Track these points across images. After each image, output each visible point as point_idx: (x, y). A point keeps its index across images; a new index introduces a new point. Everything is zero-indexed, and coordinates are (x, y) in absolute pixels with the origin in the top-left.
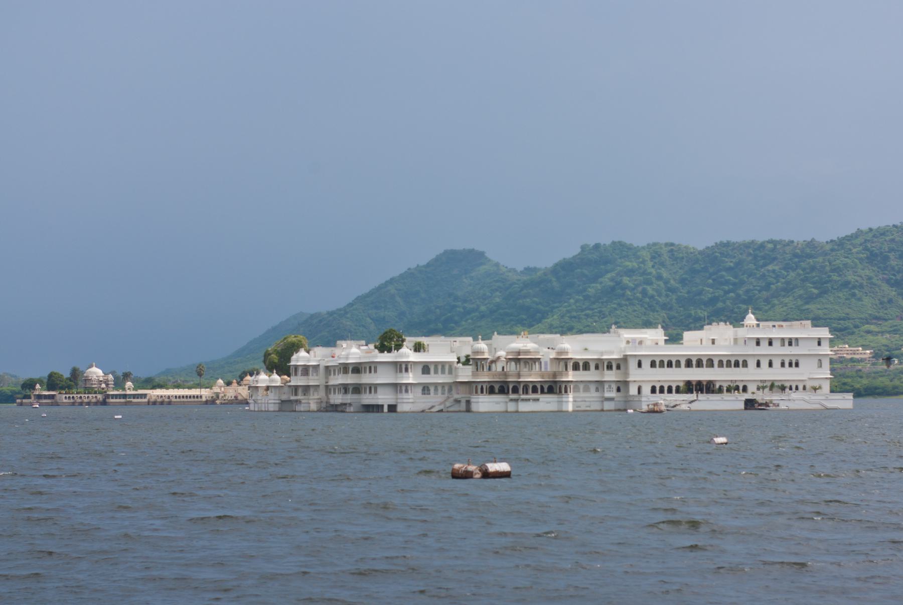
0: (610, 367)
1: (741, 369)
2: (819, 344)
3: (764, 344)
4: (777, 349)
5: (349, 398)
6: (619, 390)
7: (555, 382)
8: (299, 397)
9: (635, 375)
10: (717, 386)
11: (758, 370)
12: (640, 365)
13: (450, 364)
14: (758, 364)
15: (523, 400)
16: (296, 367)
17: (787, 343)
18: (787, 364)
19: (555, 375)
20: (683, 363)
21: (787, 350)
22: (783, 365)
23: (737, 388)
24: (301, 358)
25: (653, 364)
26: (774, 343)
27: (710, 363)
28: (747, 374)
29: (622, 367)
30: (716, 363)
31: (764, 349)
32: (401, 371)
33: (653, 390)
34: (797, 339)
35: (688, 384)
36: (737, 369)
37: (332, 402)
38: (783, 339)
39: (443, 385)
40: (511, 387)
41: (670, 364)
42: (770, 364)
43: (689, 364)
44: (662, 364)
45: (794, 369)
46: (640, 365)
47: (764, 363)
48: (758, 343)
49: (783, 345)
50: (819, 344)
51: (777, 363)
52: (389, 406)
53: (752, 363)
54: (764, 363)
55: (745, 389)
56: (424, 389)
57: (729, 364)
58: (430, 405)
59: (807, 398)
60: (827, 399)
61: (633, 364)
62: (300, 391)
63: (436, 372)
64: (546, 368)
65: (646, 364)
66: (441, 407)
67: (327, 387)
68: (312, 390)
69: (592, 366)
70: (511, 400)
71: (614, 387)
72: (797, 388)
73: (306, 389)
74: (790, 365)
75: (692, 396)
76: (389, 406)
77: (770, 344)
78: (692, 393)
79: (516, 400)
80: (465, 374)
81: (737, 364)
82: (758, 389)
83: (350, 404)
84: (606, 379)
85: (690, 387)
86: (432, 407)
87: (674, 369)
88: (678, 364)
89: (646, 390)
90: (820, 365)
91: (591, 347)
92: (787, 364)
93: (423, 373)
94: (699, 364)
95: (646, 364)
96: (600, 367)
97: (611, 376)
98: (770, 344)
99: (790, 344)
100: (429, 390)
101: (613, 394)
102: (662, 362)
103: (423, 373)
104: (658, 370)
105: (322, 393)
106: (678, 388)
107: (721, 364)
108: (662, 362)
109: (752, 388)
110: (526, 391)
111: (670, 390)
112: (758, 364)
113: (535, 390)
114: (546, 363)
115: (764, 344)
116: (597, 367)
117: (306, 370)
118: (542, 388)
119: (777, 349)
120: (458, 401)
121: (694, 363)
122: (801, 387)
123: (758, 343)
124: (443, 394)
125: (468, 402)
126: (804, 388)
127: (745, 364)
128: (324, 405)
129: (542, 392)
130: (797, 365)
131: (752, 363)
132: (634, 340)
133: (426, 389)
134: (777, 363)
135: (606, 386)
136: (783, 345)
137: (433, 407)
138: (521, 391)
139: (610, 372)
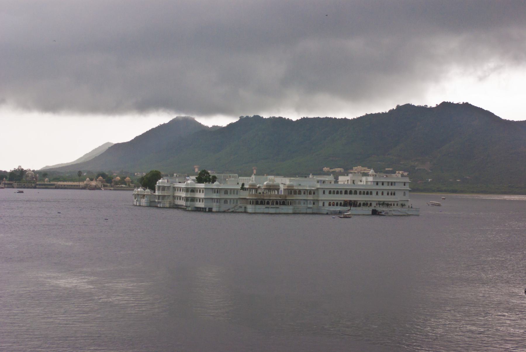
0: (310, 193)
1: (369, 195)
2: (405, 185)
3: (380, 184)
4: (386, 187)
5: (189, 203)
6: (314, 204)
7: (286, 200)
8: (160, 201)
10: (358, 204)
11: (377, 196)
12: (324, 193)
13: (237, 189)
14: (377, 194)
15: (271, 208)
16: (159, 187)
18: (390, 194)
19: (286, 197)
20: (343, 192)
22: (388, 194)
23: (367, 204)
24: (160, 182)
25: (330, 193)
26: (384, 184)
27: (356, 193)
28: (373, 198)
29: (316, 193)
30: (358, 192)
31: (380, 187)
32: (215, 192)
34: (395, 182)
35: (345, 201)
37: (176, 203)
38: (388, 182)
39: (234, 199)
40: (266, 201)
41: (337, 193)
42: (382, 194)
43: (346, 193)
45: (393, 196)
46: (324, 193)
47: (380, 193)
48: (377, 184)
50: (405, 185)
51: (385, 193)
52: (209, 208)
53: (374, 193)
54: (380, 193)
55: (371, 204)
56: (225, 201)
57: (364, 193)
58: (227, 208)
59: (399, 210)
60: (408, 210)
61: (321, 192)
62: (161, 198)
63: (231, 193)
64: (281, 193)
65: (327, 192)
66: (233, 210)
67: (174, 196)
68: (166, 197)
69: (302, 193)
70: (266, 208)
71: (312, 202)
72: (394, 205)
73: (164, 197)
74: (391, 194)
75: (348, 208)
76: (209, 208)
77: (383, 184)
78: (347, 206)
79: (268, 208)
80: (245, 195)
81: (367, 193)
82: (377, 205)
83: (189, 207)
84: (309, 198)
85: (346, 203)
86: (229, 209)
87: (339, 195)
88: (341, 193)
89: (327, 204)
90: (405, 194)
91: (302, 184)
92: (390, 194)
93: (225, 194)
94: (351, 193)
95: (327, 192)
96: (306, 193)
97: (310, 197)
98: (383, 184)
99: (392, 185)
101: (311, 206)
103: (225, 194)
104: (332, 195)
105: (171, 199)
106: (341, 203)
107: (360, 193)
108: (334, 192)
109: (374, 204)
110: (273, 204)
111: (337, 205)
112: (377, 194)
113: (277, 203)
114: (281, 191)
115: (380, 184)
116: (304, 193)
117: (164, 188)
118: (280, 203)
119: (386, 187)
120: (241, 207)
121: (348, 192)
122: (396, 205)
123: (377, 184)
124: (233, 203)
125: (245, 208)
126: (397, 205)
127: (371, 193)
128: (172, 205)
129: (280, 204)
130: (394, 194)
131: (374, 193)
132: (321, 180)
133: (226, 201)
134: (385, 193)
135: (309, 202)
137: (229, 209)
138: (270, 204)
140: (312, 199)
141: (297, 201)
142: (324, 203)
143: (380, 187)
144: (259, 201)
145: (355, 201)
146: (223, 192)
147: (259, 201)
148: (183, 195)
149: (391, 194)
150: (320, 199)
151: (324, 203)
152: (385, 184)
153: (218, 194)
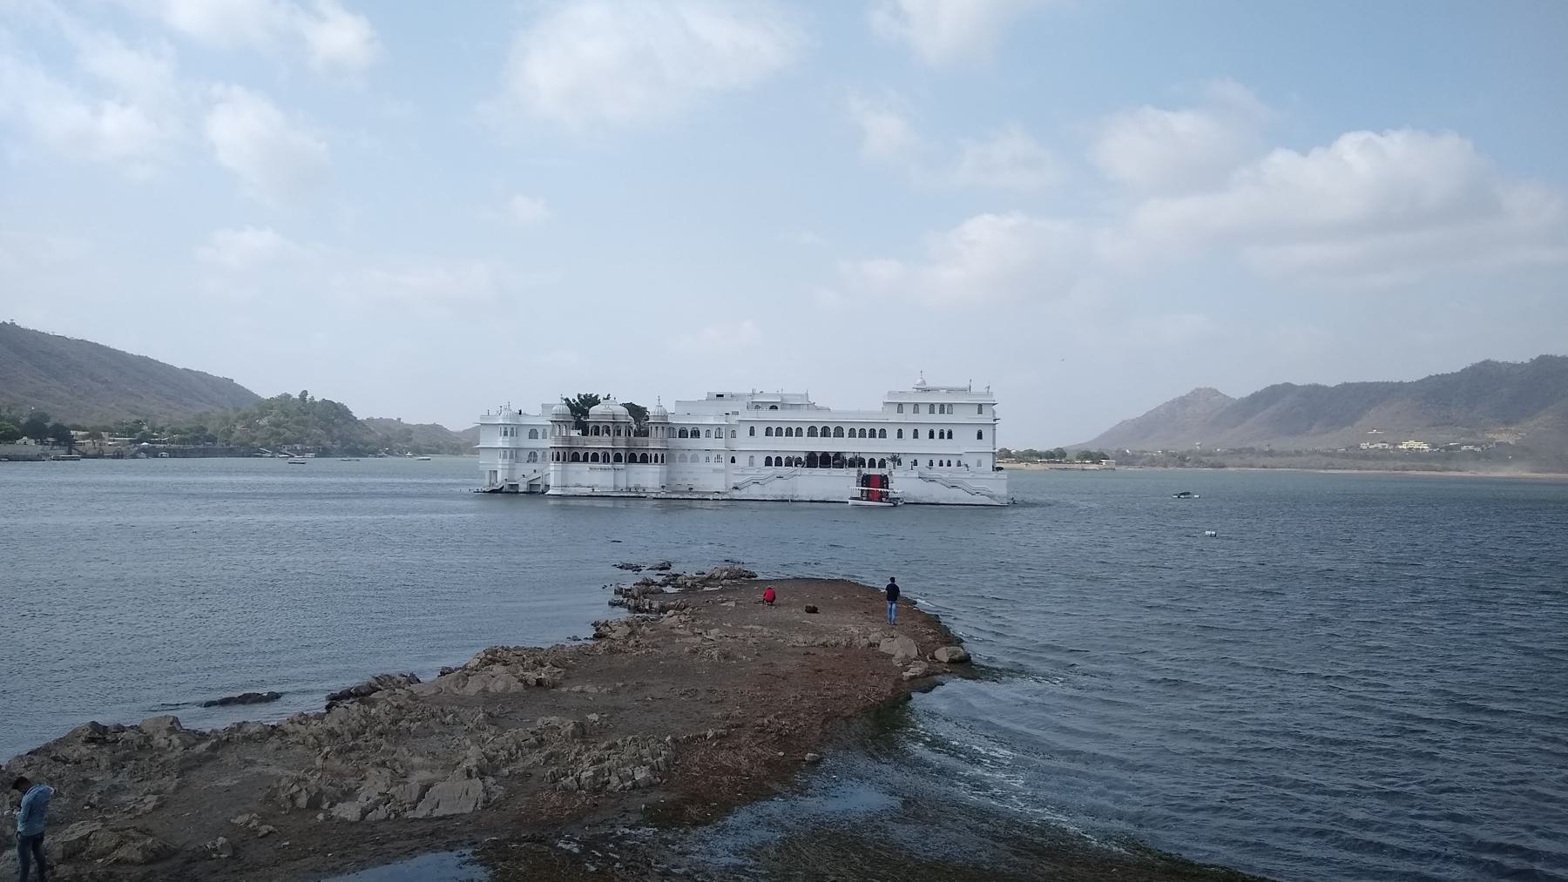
2: (980, 412)
3: (908, 410)
4: (924, 416)
12: (752, 433)
17: (937, 409)
18: (937, 435)
20: (805, 431)
21: (937, 418)
22: (932, 435)
25: (768, 432)
27: (839, 432)
30: (846, 432)
31: (909, 416)
33: (768, 462)
38: (932, 405)
41: (789, 432)
42: (916, 435)
43: (812, 432)
46: (752, 433)
47: (908, 433)
49: (932, 411)
50: (980, 412)
51: (924, 433)
53: (892, 433)
54: (908, 433)
57: (862, 433)
65: (760, 430)
69: (702, 434)
74: (942, 436)
81: (873, 434)
88: (799, 432)
92: (937, 435)
97: (719, 444)
102: (779, 430)
107: (852, 433)
108: (779, 430)
115: (908, 410)
119: (924, 416)
122: (954, 463)
127: (883, 434)
130: (950, 436)
131: (892, 433)
134: (924, 433)
136: (932, 411)
143: (909, 416)
148: (501, 442)
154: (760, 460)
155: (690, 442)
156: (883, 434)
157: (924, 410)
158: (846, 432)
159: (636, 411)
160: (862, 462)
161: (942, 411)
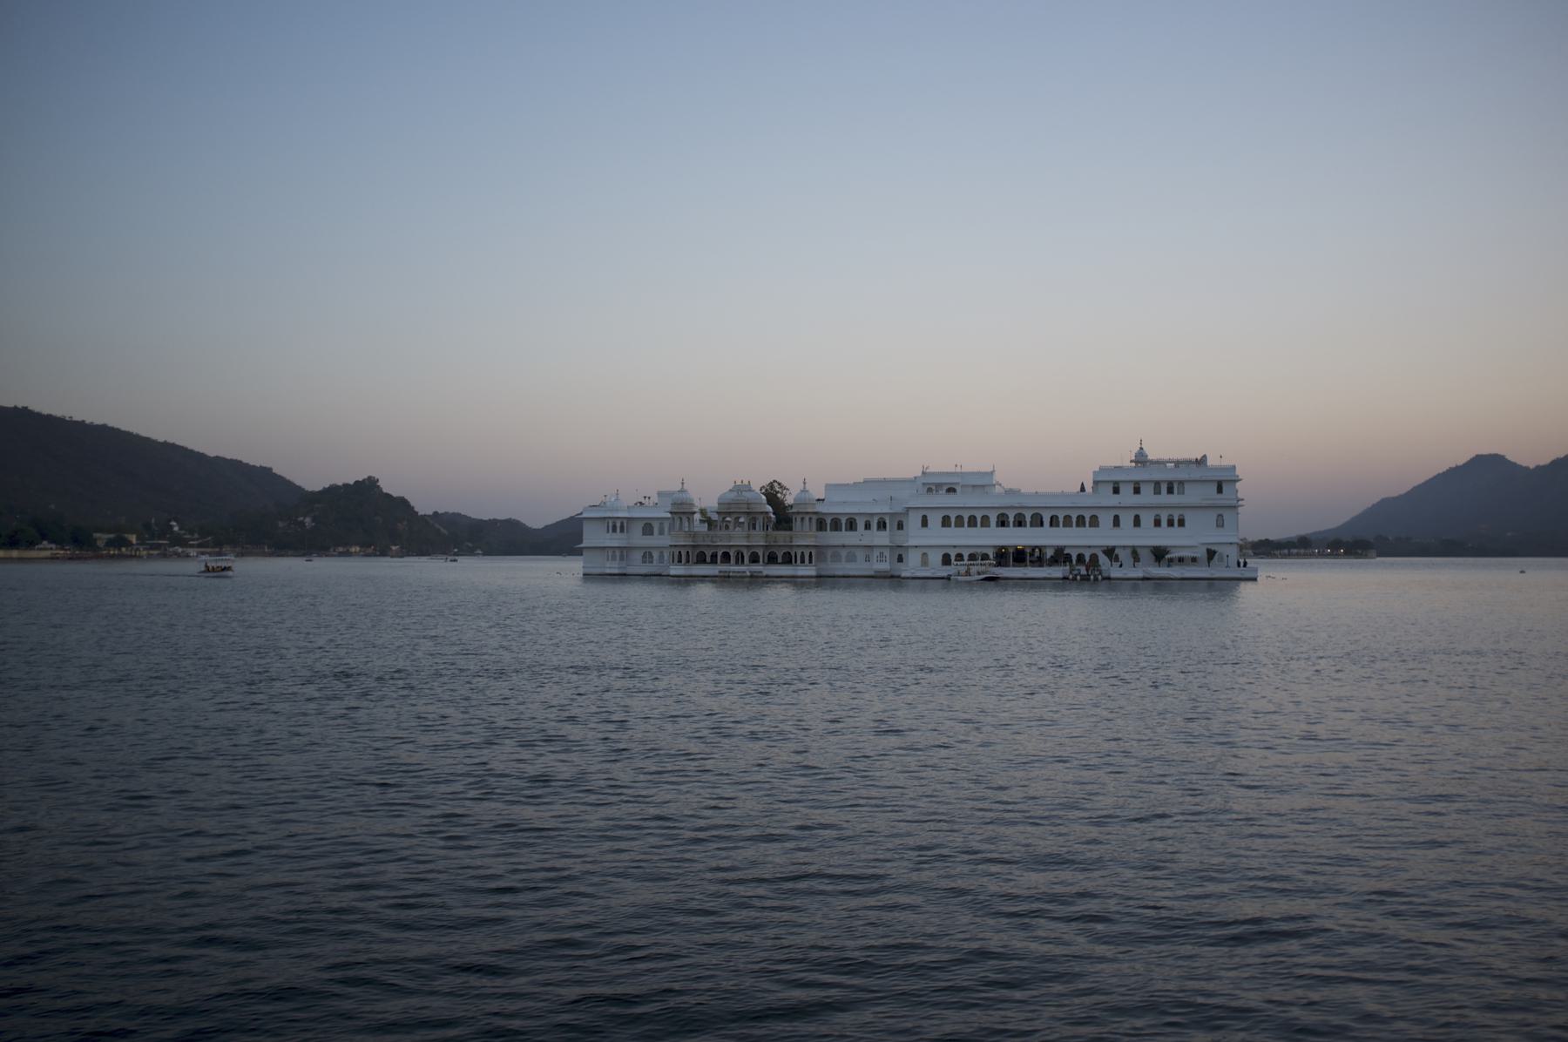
2: (1220, 490)
3: (1127, 491)
9: (914, 535)
11: (1117, 531)
12: (925, 523)
14: (1116, 522)
17: (1164, 488)
18: (1164, 523)
20: (993, 520)
21: (1164, 498)
22: (1157, 523)
25: (946, 522)
27: (1038, 521)
30: (1047, 521)
33: (946, 560)
34: (1181, 483)
36: (1081, 529)
38: (1157, 484)
41: (972, 522)
42: (1137, 522)
44: (959, 522)
46: (925, 523)
47: (1127, 519)
48: (1116, 491)
49: (1157, 491)
50: (1220, 490)
51: (1147, 519)
53: (1106, 519)
54: (1127, 519)
56: (644, 556)
57: (1068, 521)
61: (913, 521)
63: (661, 533)
65: (935, 520)
69: (861, 524)
74: (1171, 523)
77: (1137, 491)
81: (1081, 521)
84: (876, 542)
87: (979, 530)
88: (985, 521)
92: (1164, 523)
95: (935, 520)
97: (881, 538)
98: (1137, 491)
100: (651, 556)
102: (959, 520)
104: (952, 530)
107: (1054, 521)
108: (959, 520)
115: (1127, 491)
123: (1116, 491)
127: (1094, 522)
130: (1182, 523)
131: (1106, 519)
134: (1147, 519)
138: (733, 560)
139: (882, 533)
140: (886, 542)
141: (844, 553)
142: (924, 554)
144: (708, 554)
145: (1034, 548)
146: (637, 529)
147: (708, 554)
149: (1171, 523)
150: (912, 542)
151: (924, 554)
152: (1147, 490)
153: (624, 536)
154: (936, 558)
155: (844, 537)
156: (1094, 522)
157: (1147, 490)
158: (1047, 521)
159: (772, 494)
160: (1068, 558)
161: (1170, 491)
